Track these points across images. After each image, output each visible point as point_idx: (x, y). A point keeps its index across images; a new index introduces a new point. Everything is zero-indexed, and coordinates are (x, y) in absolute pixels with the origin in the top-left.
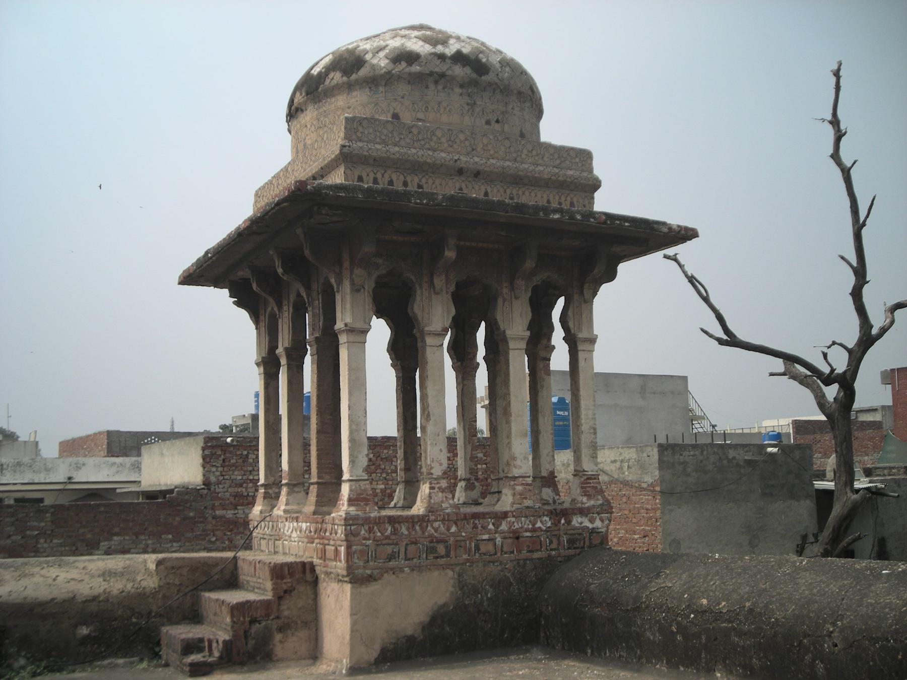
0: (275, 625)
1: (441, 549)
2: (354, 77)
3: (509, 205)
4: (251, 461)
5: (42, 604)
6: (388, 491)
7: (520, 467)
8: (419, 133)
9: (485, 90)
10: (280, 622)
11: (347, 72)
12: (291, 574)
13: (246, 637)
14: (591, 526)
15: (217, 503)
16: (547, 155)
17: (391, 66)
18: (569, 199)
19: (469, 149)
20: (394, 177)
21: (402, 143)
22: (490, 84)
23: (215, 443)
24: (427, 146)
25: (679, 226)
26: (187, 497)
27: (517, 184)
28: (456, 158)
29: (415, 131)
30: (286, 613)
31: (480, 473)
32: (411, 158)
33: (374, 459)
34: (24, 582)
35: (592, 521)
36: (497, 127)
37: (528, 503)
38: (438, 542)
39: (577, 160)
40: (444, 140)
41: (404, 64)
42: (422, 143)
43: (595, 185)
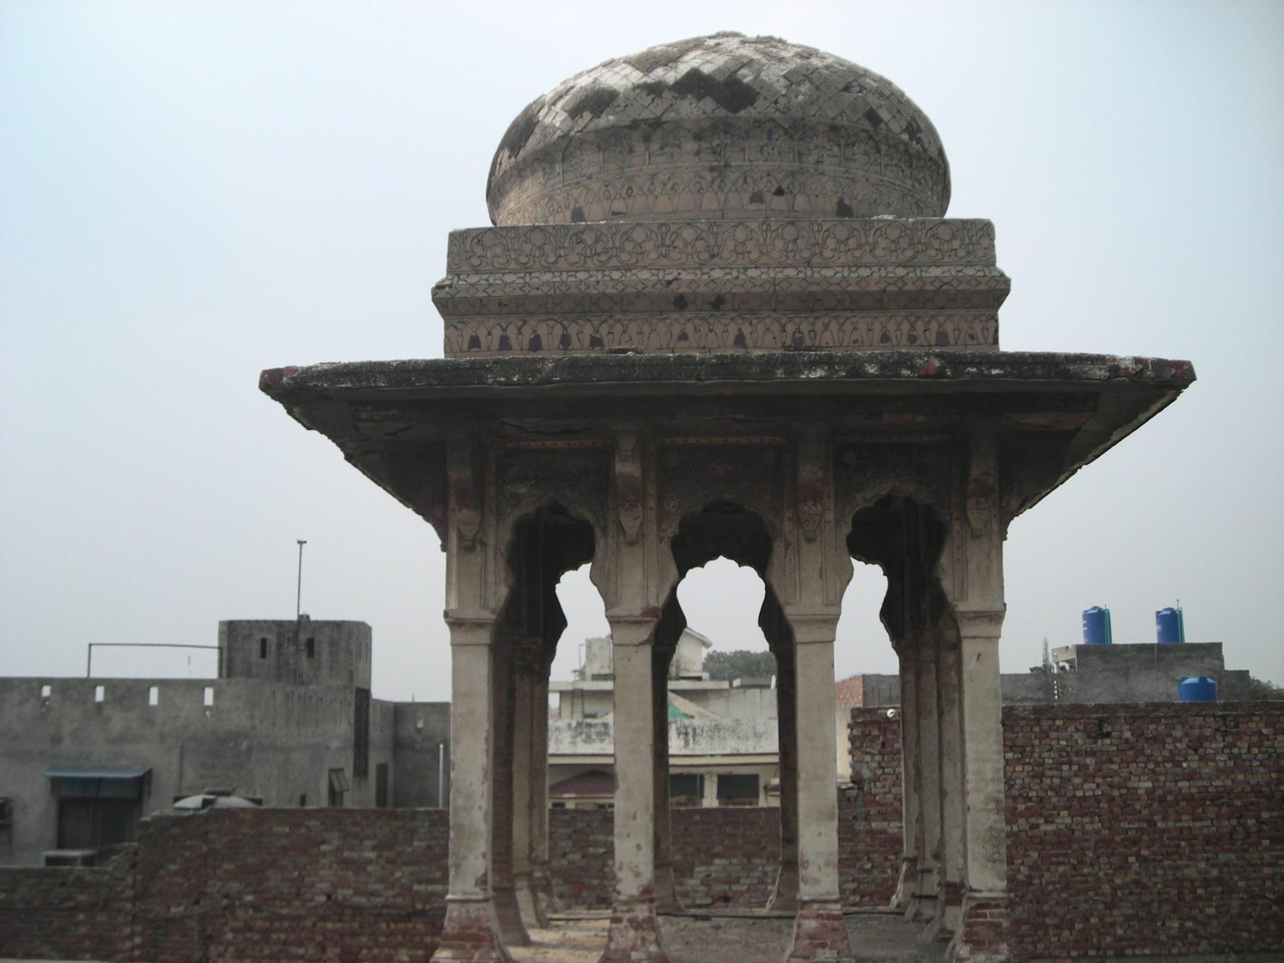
2: (522, 153)
3: (702, 361)
6: (1159, 792)
7: (817, 881)
8: (597, 241)
9: (748, 135)
15: (873, 811)
16: (882, 243)
17: (570, 123)
18: (934, 326)
19: (705, 256)
20: (542, 330)
21: (562, 264)
22: (758, 123)
23: (868, 717)
24: (614, 262)
25: (1138, 361)
27: (812, 310)
28: (670, 278)
29: (589, 238)
32: (573, 290)
33: (1133, 739)
36: (779, 203)
39: (956, 244)
40: (649, 246)
41: (587, 115)
42: (603, 258)
43: (999, 290)
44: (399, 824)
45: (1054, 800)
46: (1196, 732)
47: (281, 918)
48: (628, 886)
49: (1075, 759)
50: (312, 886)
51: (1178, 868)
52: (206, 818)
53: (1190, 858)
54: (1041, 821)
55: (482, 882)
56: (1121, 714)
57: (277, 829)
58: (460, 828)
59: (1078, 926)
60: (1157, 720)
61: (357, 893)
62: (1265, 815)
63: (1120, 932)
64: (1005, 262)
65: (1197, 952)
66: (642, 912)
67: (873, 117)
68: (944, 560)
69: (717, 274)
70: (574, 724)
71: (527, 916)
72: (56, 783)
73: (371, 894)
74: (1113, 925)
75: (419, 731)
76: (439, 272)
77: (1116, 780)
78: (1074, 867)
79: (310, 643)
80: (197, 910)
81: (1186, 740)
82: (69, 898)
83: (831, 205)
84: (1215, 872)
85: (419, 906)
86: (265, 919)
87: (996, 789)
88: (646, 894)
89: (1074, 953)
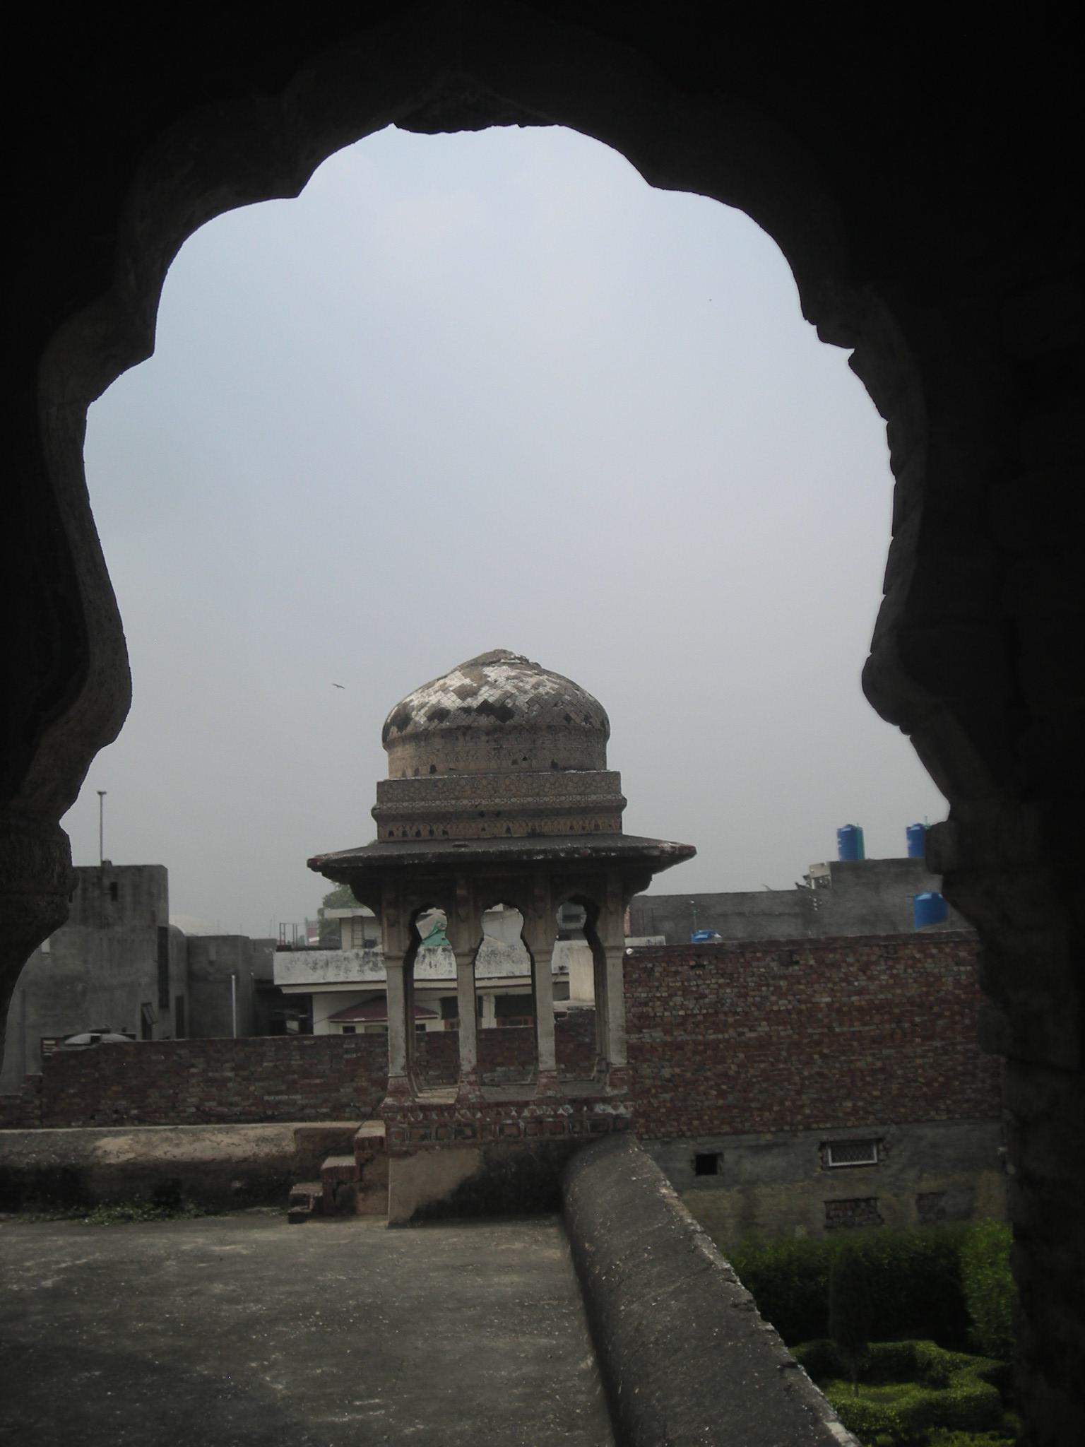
1: (468, 1132)
4: (657, 974)
6: (837, 1005)
11: (400, 729)
13: (334, 1196)
14: (614, 1112)
20: (421, 828)
22: (515, 727)
26: (581, 1020)
30: (368, 1177)
31: (964, 977)
34: (197, 1145)
35: (615, 1108)
36: (524, 764)
37: (550, 1093)
38: (466, 1125)
40: (467, 788)
43: (622, 804)
45: (756, 1013)
46: (865, 958)
49: (771, 982)
51: (851, 1062)
53: (860, 1054)
54: (746, 1030)
55: (403, 1068)
56: (807, 946)
57: (154, 1058)
58: (393, 1046)
59: (776, 1108)
60: (834, 950)
61: (220, 1104)
62: (917, 1019)
63: (808, 1111)
64: (625, 791)
65: (867, 1125)
66: (473, 1078)
67: (568, 718)
68: (599, 924)
69: (497, 800)
70: (361, 953)
73: (231, 1104)
74: (802, 1106)
75: (211, 963)
76: (373, 801)
77: (804, 997)
78: (772, 1064)
79: (114, 888)
81: (857, 965)
83: (548, 763)
84: (879, 1064)
85: (269, 1112)
87: (622, 1022)
88: (474, 1071)
89: (773, 1129)
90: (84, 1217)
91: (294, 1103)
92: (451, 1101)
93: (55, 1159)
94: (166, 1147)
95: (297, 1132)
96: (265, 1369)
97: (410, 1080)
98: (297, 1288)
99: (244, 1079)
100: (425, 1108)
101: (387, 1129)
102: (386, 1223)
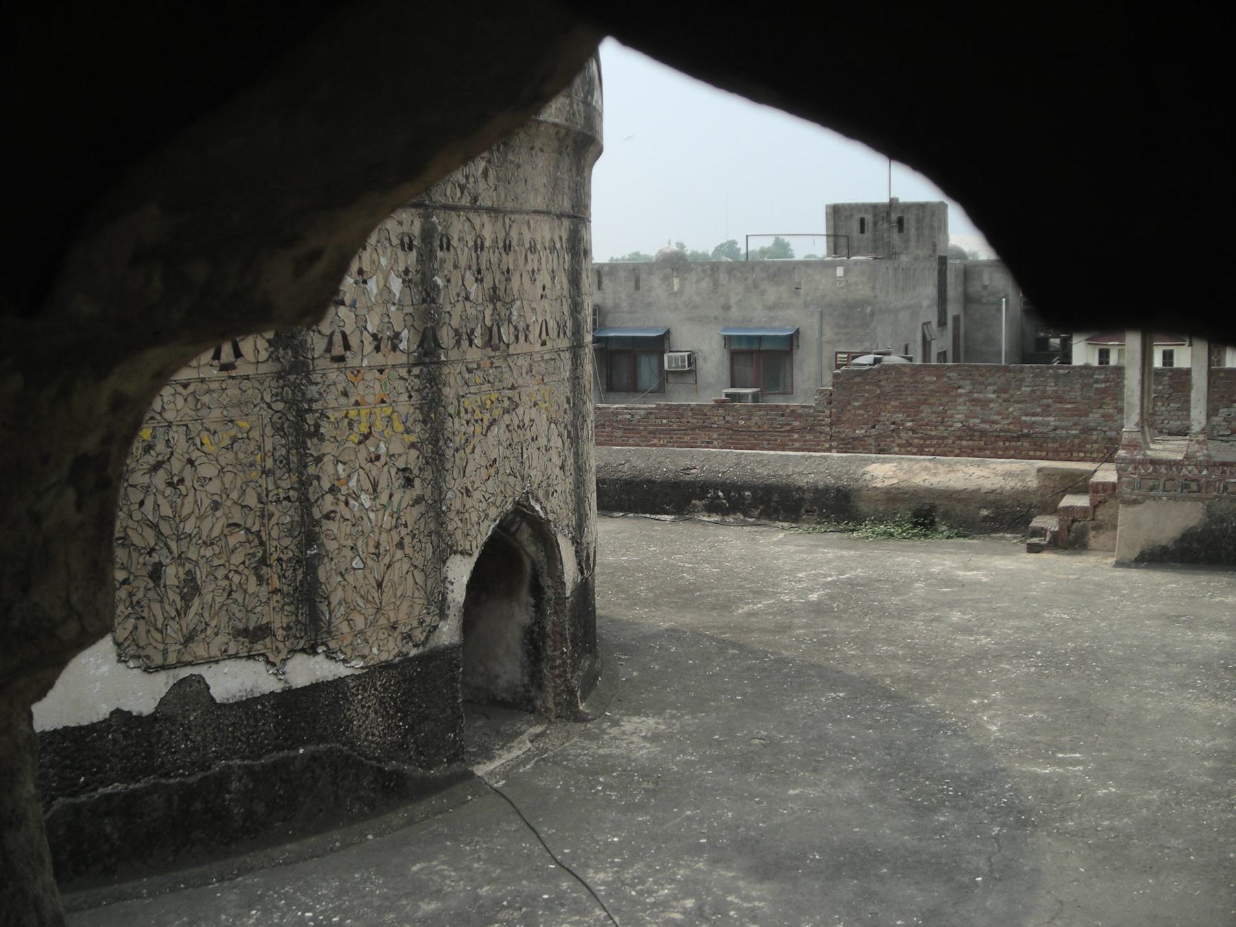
0: (1090, 524)
1: (1194, 486)
5: (958, 492)
10: (1094, 523)
12: (1104, 491)
34: (951, 475)
38: (1193, 480)
44: (1012, 375)
47: (931, 438)
48: (1196, 428)
50: (952, 417)
52: (879, 371)
55: (1137, 424)
57: (927, 378)
58: (1129, 403)
61: (982, 422)
66: (1201, 437)
71: (1149, 439)
72: (728, 340)
73: (993, 422)
75: (985, 287)
79: (900, 222)
80: (873, 432)
82: (787, 424)
85: (1026, 431)
86: (920, 438)
88: (1203, 431)
90: (853, 531)
91: (1048, 424)
92: (1180, 457)
93: (831, 481)
94: (925, 476)
95: (1039, 470)
96: (985, 708)
97: (1143, 433)
98: (1025, 623)
99: (1005, 401)
100: (1154, 462)
101: (1119, 478)
102: (1114, 560)
